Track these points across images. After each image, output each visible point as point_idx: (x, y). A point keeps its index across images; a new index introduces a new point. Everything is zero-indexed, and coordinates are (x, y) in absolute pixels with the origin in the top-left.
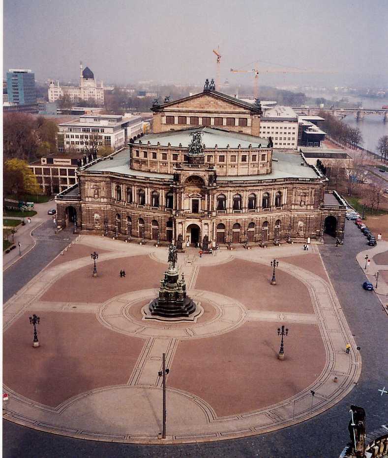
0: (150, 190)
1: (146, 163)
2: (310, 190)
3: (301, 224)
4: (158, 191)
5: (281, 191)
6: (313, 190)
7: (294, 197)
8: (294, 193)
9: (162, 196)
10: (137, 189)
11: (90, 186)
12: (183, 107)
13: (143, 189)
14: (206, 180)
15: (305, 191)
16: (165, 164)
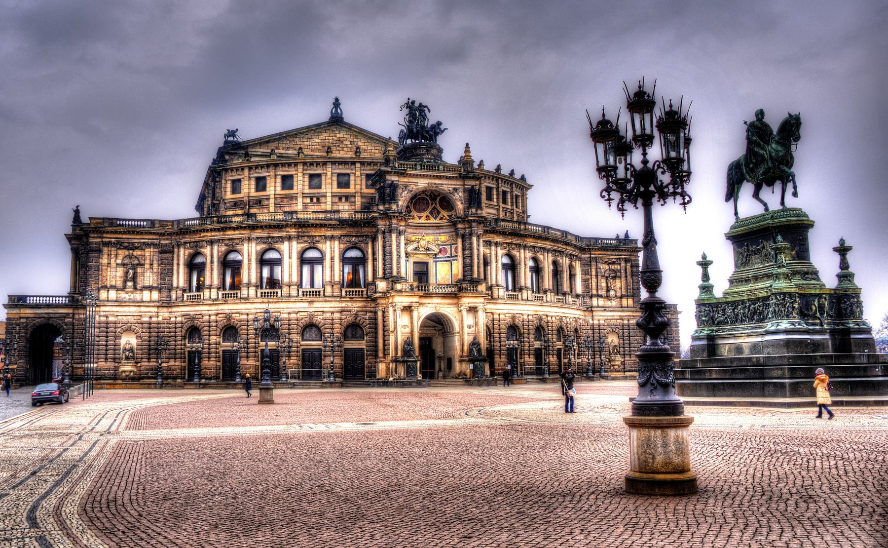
0: (296, 246)
1: (266, 202)
2: (623, 264)
3: (613, 340)
4: (320, 246)
5: (573, 263)
6: (629, 265)
7: (594, 279)
8: (594, 273)
9: (332, 258)
10: (259, 248)
11: (116, 256)
12: (288, 149)
13: (277, 246)
14: (459, 203)
15: (613, 267)
16: (318, 199)
